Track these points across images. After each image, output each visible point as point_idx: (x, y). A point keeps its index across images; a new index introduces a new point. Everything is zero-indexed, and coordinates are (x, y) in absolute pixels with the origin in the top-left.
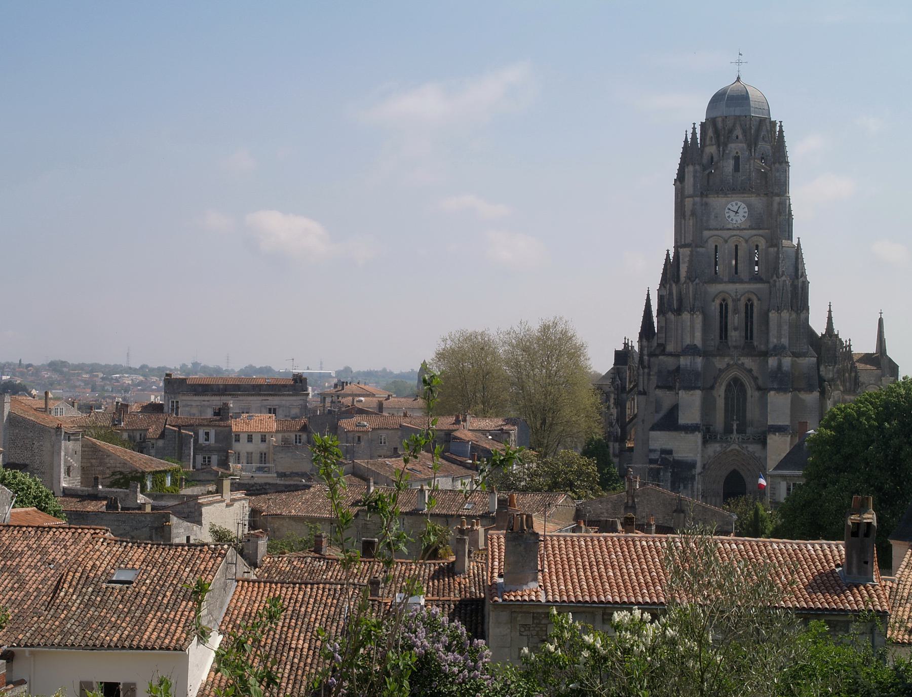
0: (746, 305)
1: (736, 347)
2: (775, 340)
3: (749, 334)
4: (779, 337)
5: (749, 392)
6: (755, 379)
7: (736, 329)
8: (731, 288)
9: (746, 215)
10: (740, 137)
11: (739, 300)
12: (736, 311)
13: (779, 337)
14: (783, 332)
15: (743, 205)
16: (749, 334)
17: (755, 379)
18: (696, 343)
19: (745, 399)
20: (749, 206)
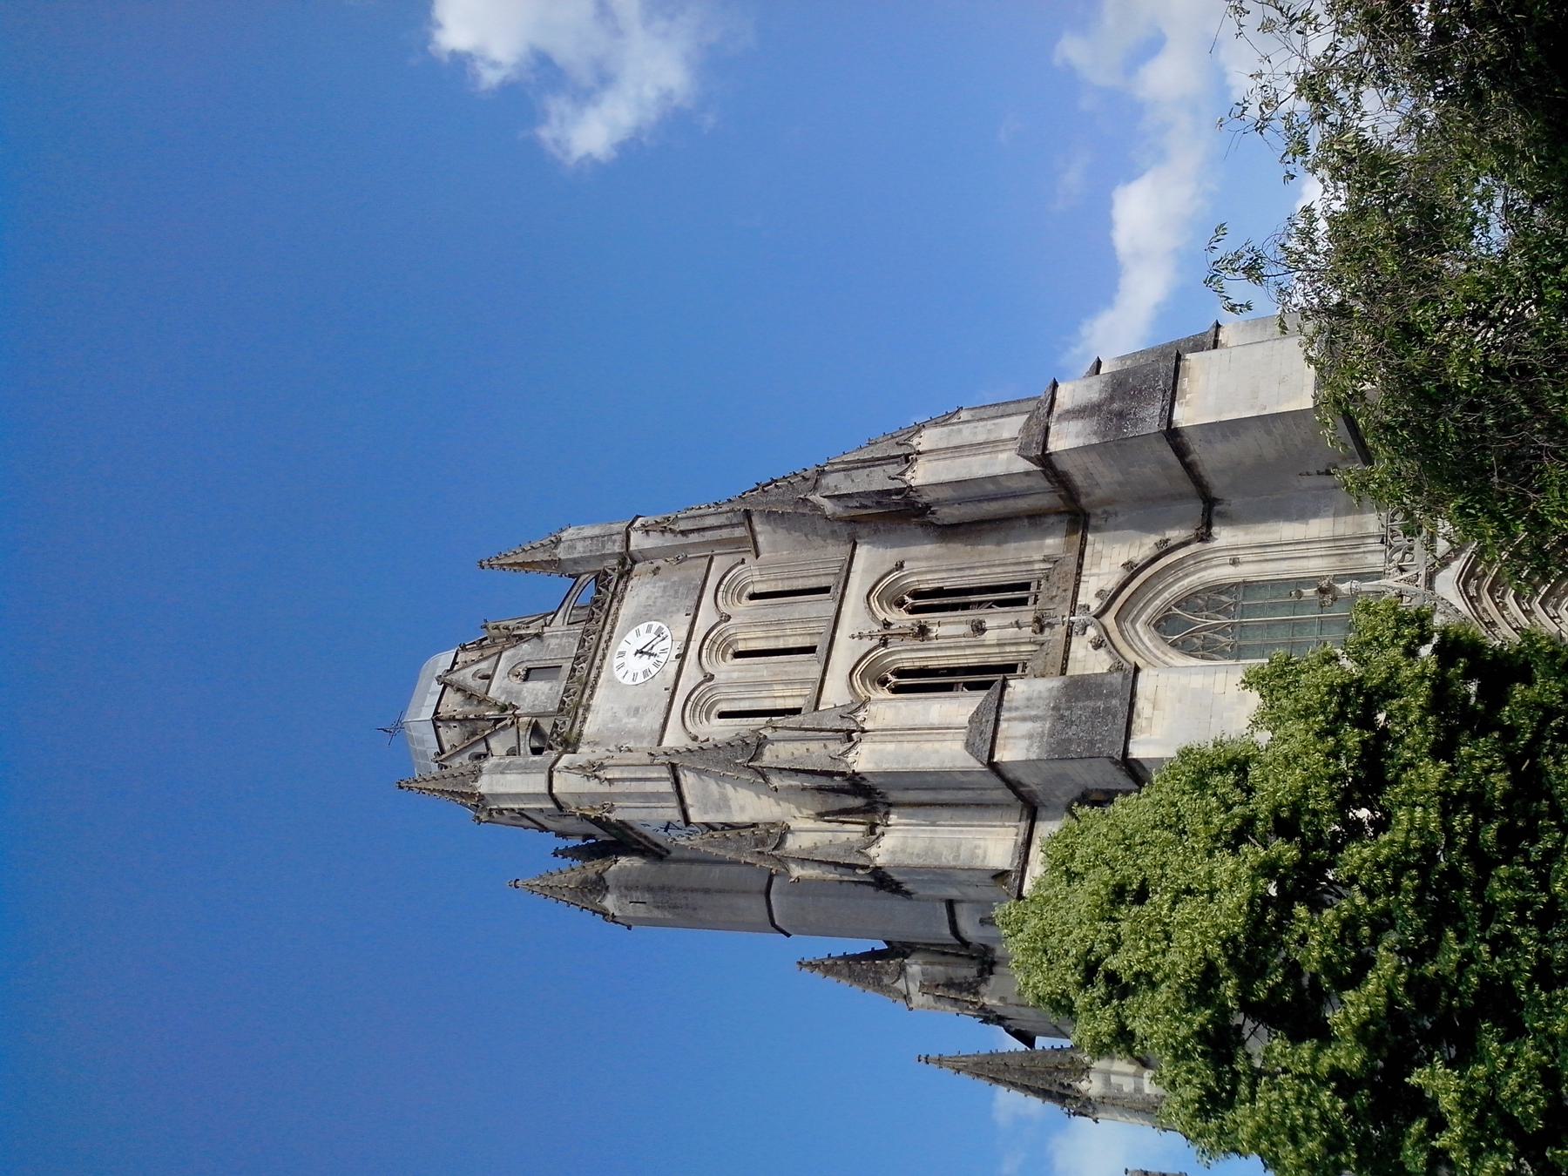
0: (914, 610)
1: (1040, 624)
2: (1003, 456)
3: (1011, 594)
4: (993, 445)
5: (1223, 573)
6: (1165, 549)
7: (979, 628)
8: (845, 654)
9: (656, 625)
10: (484, 666)
11: (887, 624)
12: (923, 631)
13: (993, 445)
14: (981, 438)
15: (631, 636)
16: (1011, 594)
17: (1165, 549)
18: (964, 719)
19: (1247, 586)
20: (637, 620)
